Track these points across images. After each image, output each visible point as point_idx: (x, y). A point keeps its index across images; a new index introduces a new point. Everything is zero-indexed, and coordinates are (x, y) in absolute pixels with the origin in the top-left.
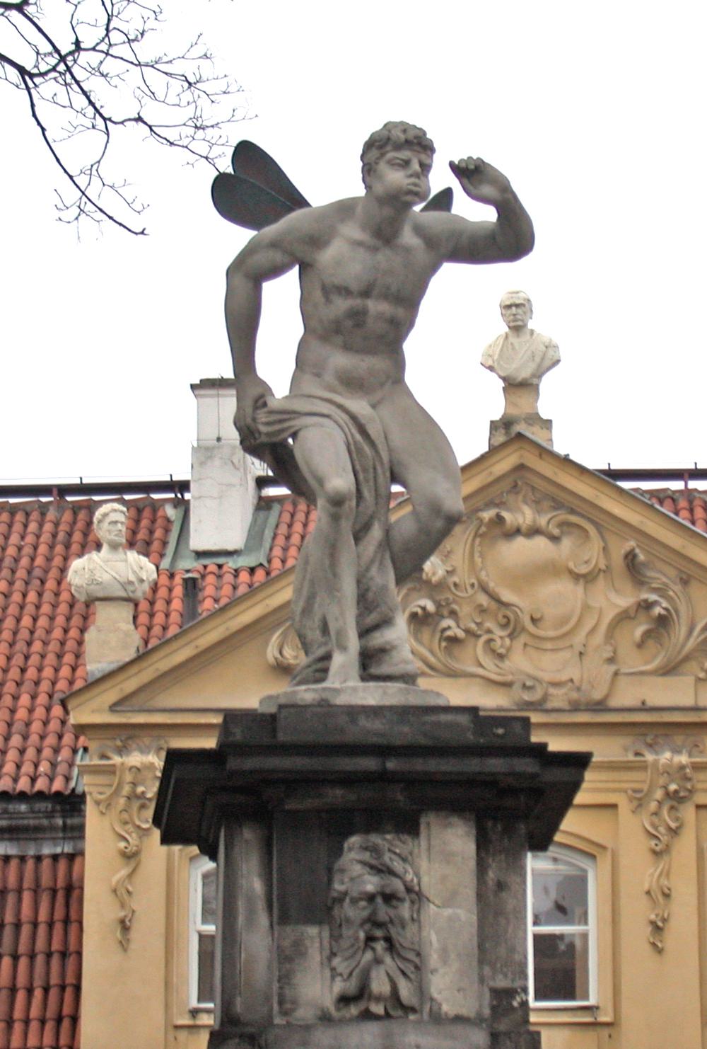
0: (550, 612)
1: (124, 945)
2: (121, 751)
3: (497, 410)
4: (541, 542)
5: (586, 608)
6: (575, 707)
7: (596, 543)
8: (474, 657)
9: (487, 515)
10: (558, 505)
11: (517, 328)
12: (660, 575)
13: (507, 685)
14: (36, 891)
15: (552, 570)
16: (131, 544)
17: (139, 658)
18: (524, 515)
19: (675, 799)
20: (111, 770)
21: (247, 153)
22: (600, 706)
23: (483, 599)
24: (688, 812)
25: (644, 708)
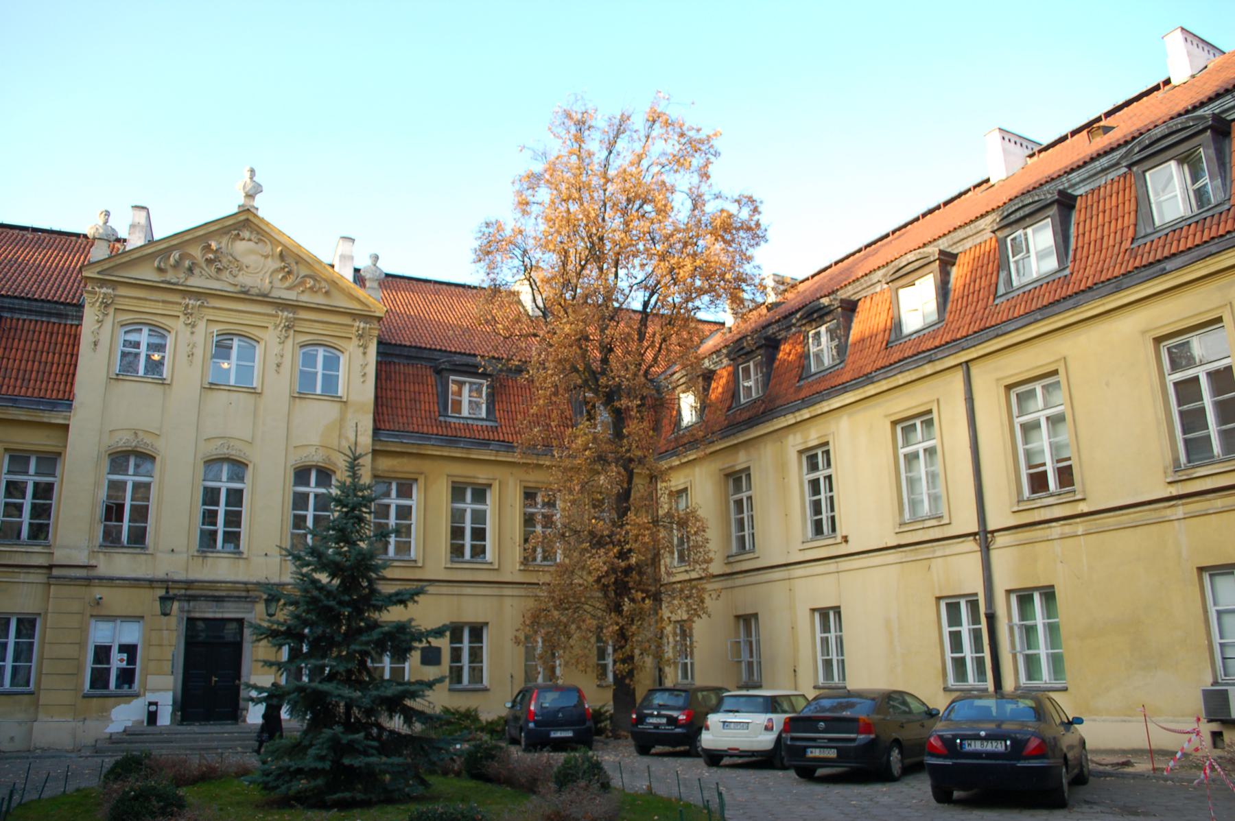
1: (94, 350)
2: (101, 287)
4: (251, 244)
5: (264, 265)
6: (258, 295)
8: (225, 275)
12: (290, 260)
13: (236, 285)
15: (252, 252)
17: (110, 258)
18: (246, 234)
19: (288, 328)
22: (266, 296)
23: (231, 258)
24: (292, 332)
25: (280, 298)
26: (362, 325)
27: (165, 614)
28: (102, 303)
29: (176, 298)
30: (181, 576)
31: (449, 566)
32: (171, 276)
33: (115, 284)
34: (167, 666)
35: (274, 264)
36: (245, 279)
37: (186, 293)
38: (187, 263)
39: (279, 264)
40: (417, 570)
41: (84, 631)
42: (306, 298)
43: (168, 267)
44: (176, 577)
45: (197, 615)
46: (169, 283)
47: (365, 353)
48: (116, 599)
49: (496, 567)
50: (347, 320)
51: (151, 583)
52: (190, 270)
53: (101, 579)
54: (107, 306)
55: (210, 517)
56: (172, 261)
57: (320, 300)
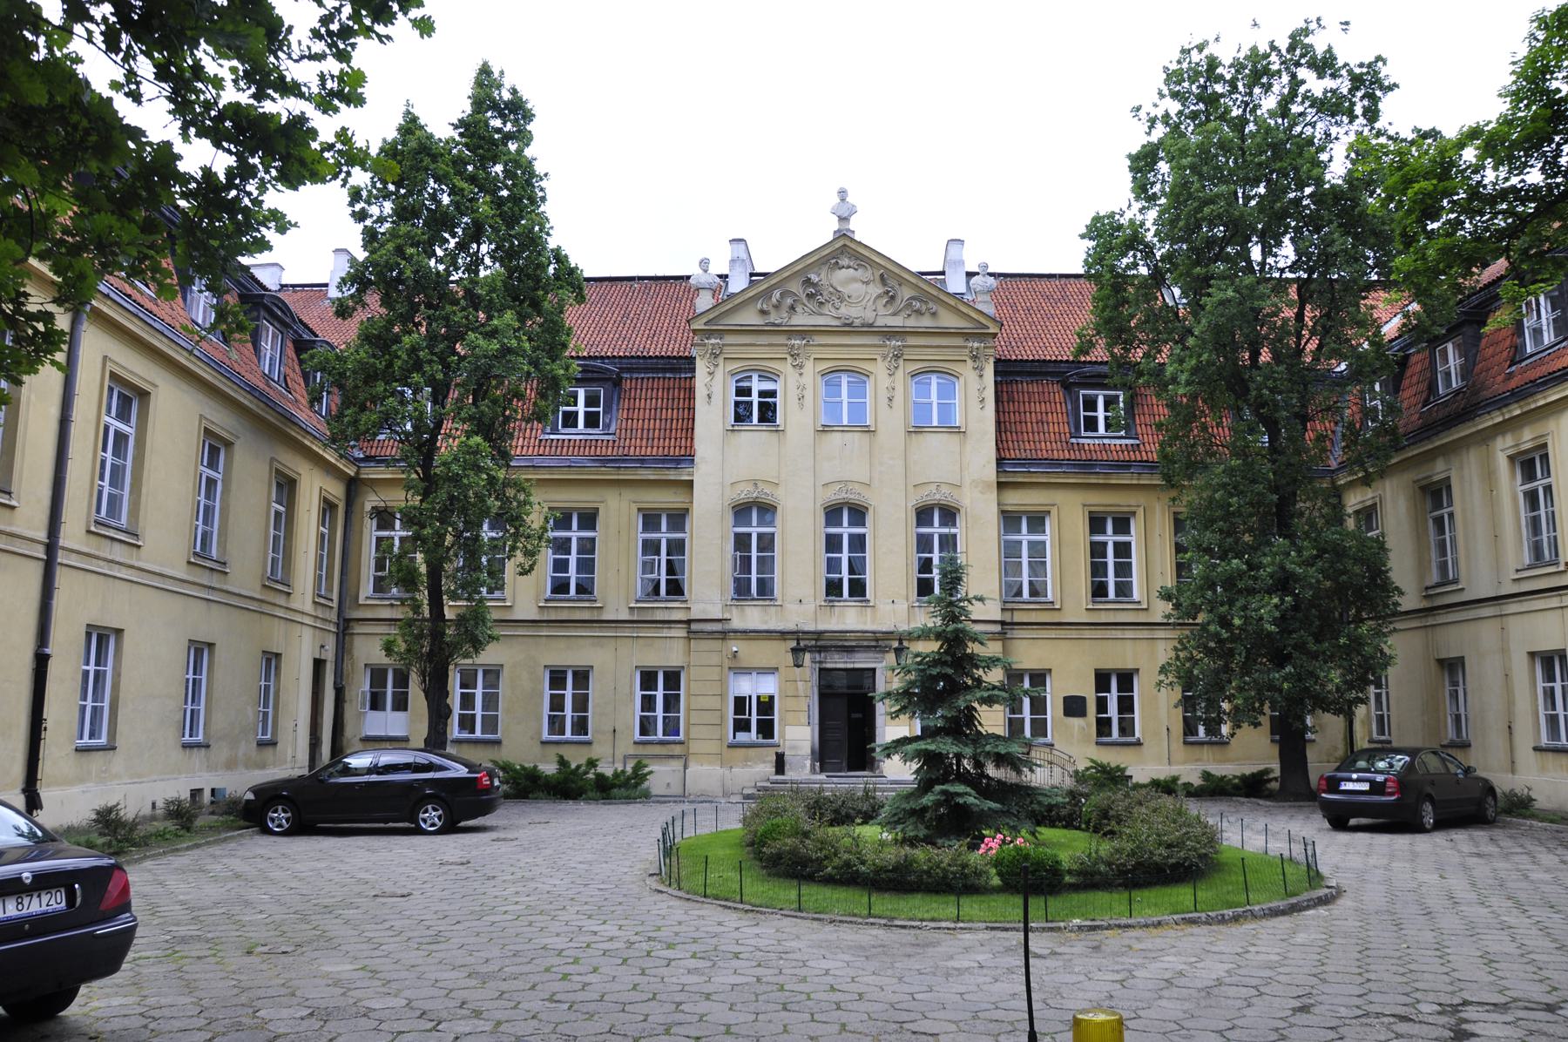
0: (854, 295)
1: (709, 403)
3: (836, 227)
4: (851, 270)
6: (863, 326)
7: (870, 272)
8: (828, 309)
10: (857, 259)
11: (843, 200)
12: (891, 282)
14: (679, 389)
15: (854, 280)
18: (845, 261)
19: (897, 357)
22: (871, 325)
24: (901, 362)
26: (976, 345)
27: (798, 666)
28: (712, 354)
29: (781, 339)
30: (811, 627)
31: (1090, 607)
32: (774, 318)
33: (721, 333)
34: (804, 718)
35: (879, 290)
37: (791, 333)
38: (789, 301)
39: (879, 290)
40: (1056, 613)
41: (723, 682)
42: (912, 322)
43: (771, 308)
44: (806, 628)
45: (829, 666)
46: (774, 325)
47: (981, 376)
48: (750, 652)
49: (1145, 606)
50: (959, 341)
51: (783, 635)
52: (792, 308)
53: (735, 632)
54: (716, 356)
55: (833, 565)
56: (774, 300)
57: (926, 322)
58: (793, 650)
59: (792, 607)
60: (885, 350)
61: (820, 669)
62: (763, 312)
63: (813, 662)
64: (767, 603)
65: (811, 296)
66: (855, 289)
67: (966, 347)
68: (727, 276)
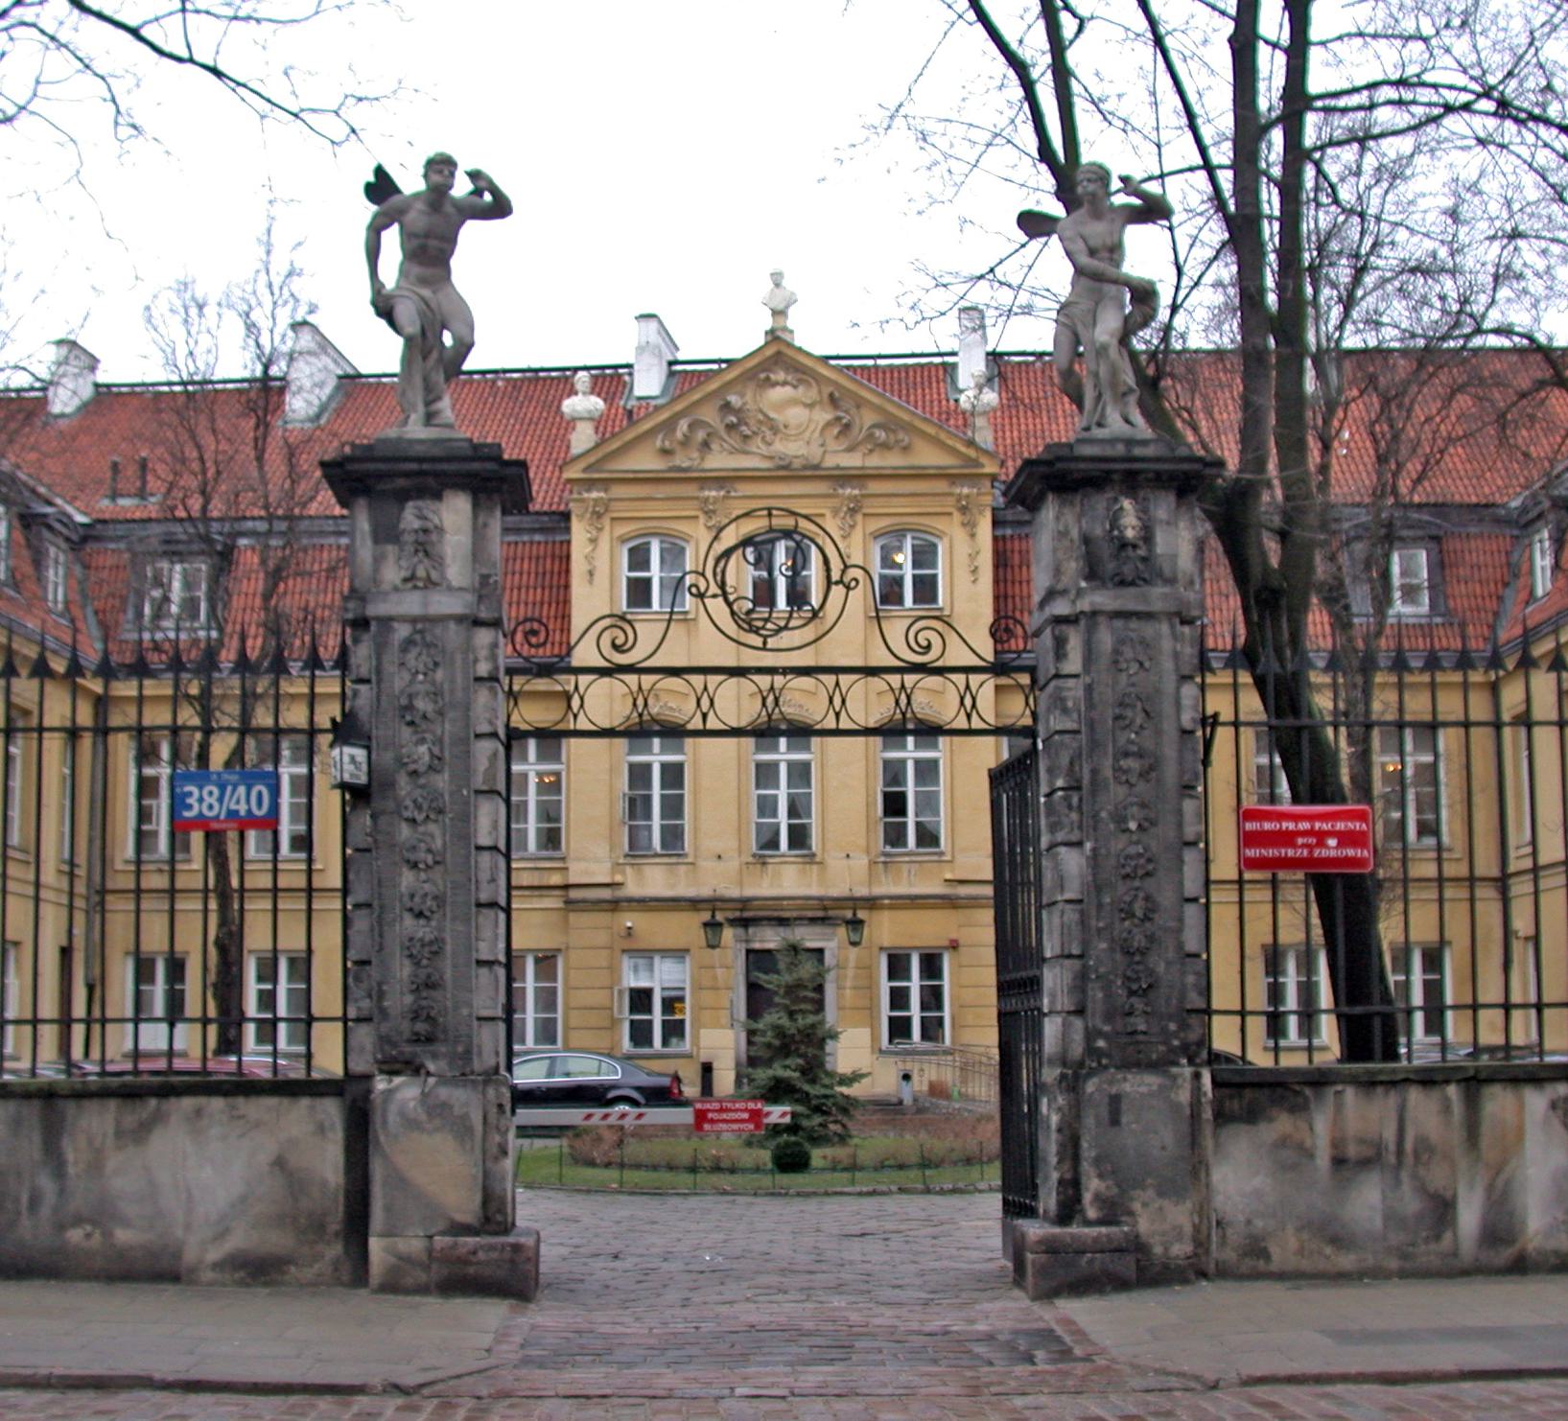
0: (793, 422)
1: (591, 582)
2: (589, 490)
3: (768, 323)
4: (788, 389)
8: (757, 445)
9: (762, 376)
11: (777, 285)
13: (771, 458)
14: (553, 557)
15: (793, 402)
16: (592, 392)
17: (597, 446)
19: (853, 511)
20: (583, 500)
21: (380, 172)
22: (817, 467)
23: (761, 417)
24: (859, 518)
25: (838, 468)
26: (966, 491)
27: (712, 947)
28: (594, 512)
29: (690, 490)
30: (734, 892)
33: (606, 483)
34: (725, 1019)
35: (824, 416)
36: (791, 449)
37: (704, 481)
38: (701, 435)
41: (614, 970)
42: (875, 461)
45: (757, 946)
47: (973, 536)
48: (649, 927)
50: (941, 486)
51: (694, 904)
52: (706, 445)
53: (630, 900)
54: (599, 516)
55: (767, 807)
56: (679, 435)
57: (893, 460)
58: (706, 925)
59: (707, 864)
60: (835, 502)
61: (749, 952)
62: (666, 452)
63: (738, 940)
64: (674, 860)
65: (730, 427)
66: (796, 415)
67: (951, 494)
68: (629, 366)
